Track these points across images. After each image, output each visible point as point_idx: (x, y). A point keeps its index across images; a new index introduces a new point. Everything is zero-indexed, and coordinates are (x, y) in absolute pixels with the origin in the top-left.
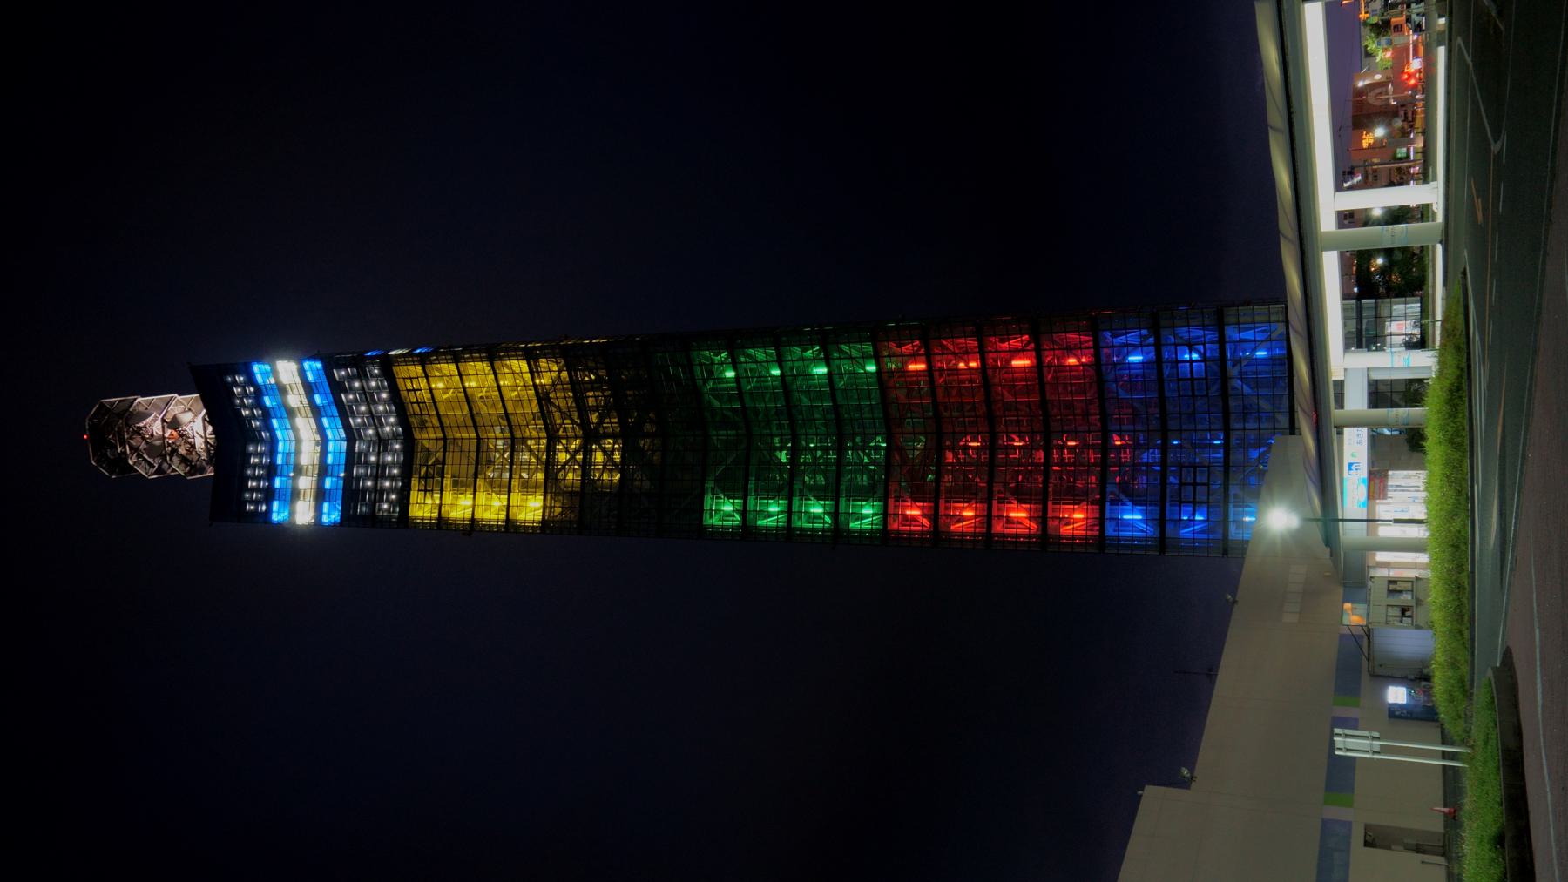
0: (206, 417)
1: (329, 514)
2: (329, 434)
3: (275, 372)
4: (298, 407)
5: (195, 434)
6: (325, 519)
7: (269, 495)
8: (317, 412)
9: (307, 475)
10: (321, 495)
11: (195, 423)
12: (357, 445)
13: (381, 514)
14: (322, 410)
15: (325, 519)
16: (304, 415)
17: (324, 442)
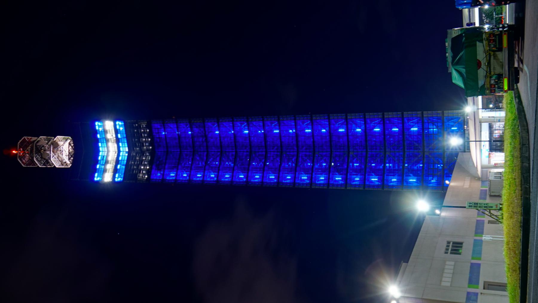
1: (118, 179)
2: (121, 149)
3: (103, 126)
4: (111, 139)
5: (63, 150)
6: (116, 180)
7: (95, 170)
8: (118, 141)
9: (110, 164)
10: (115, 171)
11: (64, 146)
12: (132, 153)
13: (139, 178)
14: (120, 140)
15: (116, 180)
16: (112, 141)
17: (119, 151)
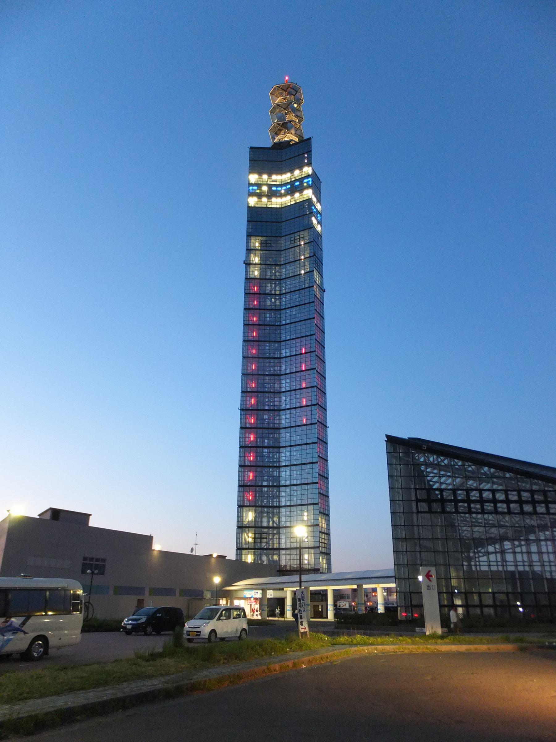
0: (294, 142)
